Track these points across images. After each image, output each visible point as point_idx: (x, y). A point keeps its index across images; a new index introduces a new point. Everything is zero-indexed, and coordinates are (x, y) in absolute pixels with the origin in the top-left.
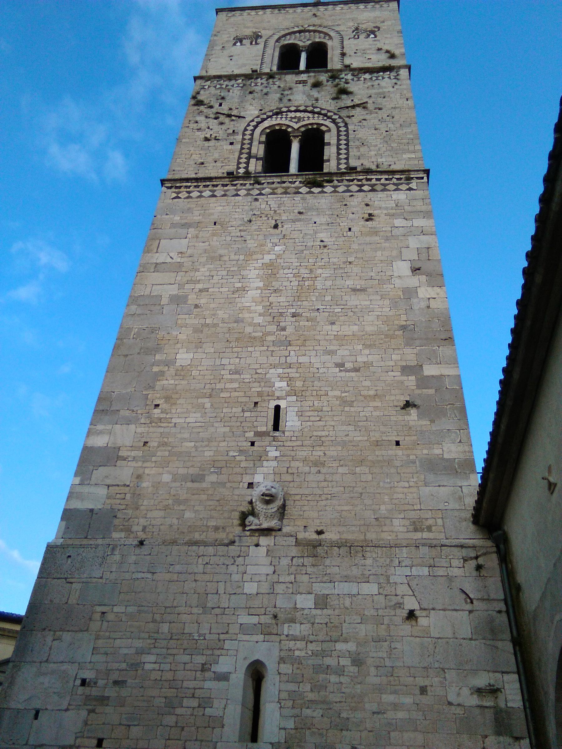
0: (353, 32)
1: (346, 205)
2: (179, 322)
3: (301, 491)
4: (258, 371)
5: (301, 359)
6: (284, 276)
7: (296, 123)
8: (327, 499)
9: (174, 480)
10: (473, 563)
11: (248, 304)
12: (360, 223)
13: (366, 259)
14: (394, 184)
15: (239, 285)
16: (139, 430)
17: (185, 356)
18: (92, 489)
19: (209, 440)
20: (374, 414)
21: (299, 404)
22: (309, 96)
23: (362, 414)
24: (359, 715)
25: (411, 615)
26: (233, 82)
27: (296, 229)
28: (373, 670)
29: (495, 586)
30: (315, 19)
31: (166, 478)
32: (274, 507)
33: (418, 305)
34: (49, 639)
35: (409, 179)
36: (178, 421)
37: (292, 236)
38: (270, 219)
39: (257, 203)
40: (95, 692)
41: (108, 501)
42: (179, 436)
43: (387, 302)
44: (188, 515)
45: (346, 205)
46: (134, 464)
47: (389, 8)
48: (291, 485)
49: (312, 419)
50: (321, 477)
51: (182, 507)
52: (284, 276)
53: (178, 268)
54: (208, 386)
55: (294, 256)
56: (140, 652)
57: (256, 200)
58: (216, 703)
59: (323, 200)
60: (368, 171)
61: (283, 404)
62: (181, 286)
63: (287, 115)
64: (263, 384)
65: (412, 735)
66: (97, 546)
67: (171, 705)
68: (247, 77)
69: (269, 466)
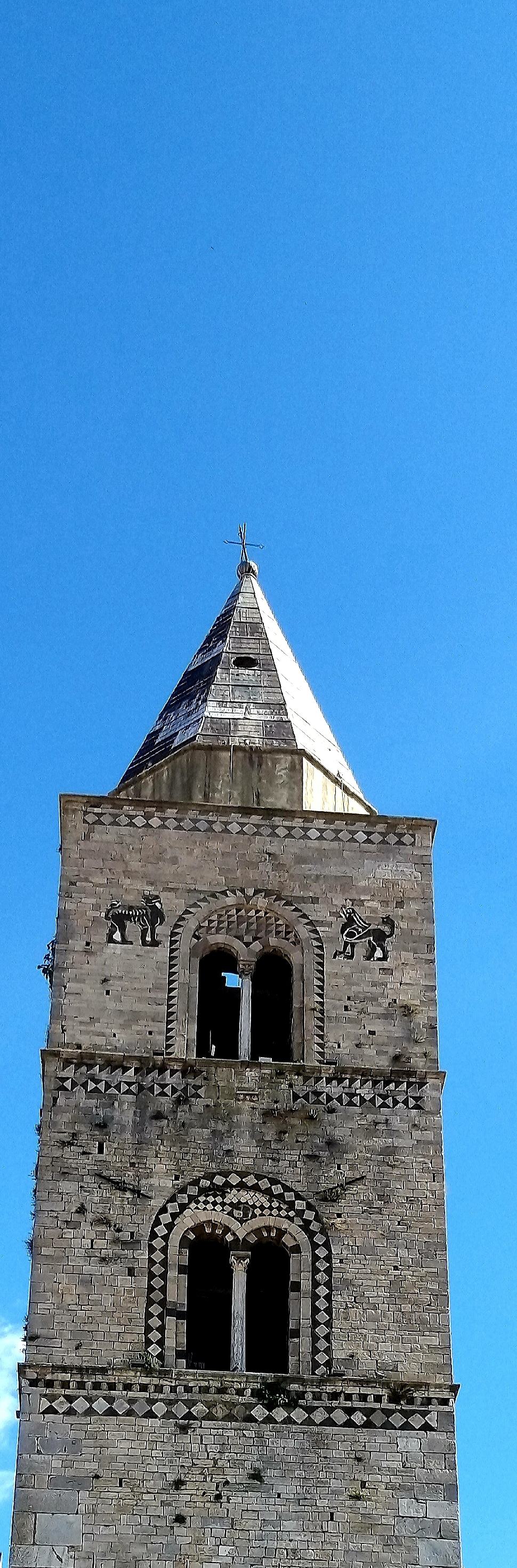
0: (342, 932)
7: (241, 1221)
26: (118, 1076)
68: (145, 1066)
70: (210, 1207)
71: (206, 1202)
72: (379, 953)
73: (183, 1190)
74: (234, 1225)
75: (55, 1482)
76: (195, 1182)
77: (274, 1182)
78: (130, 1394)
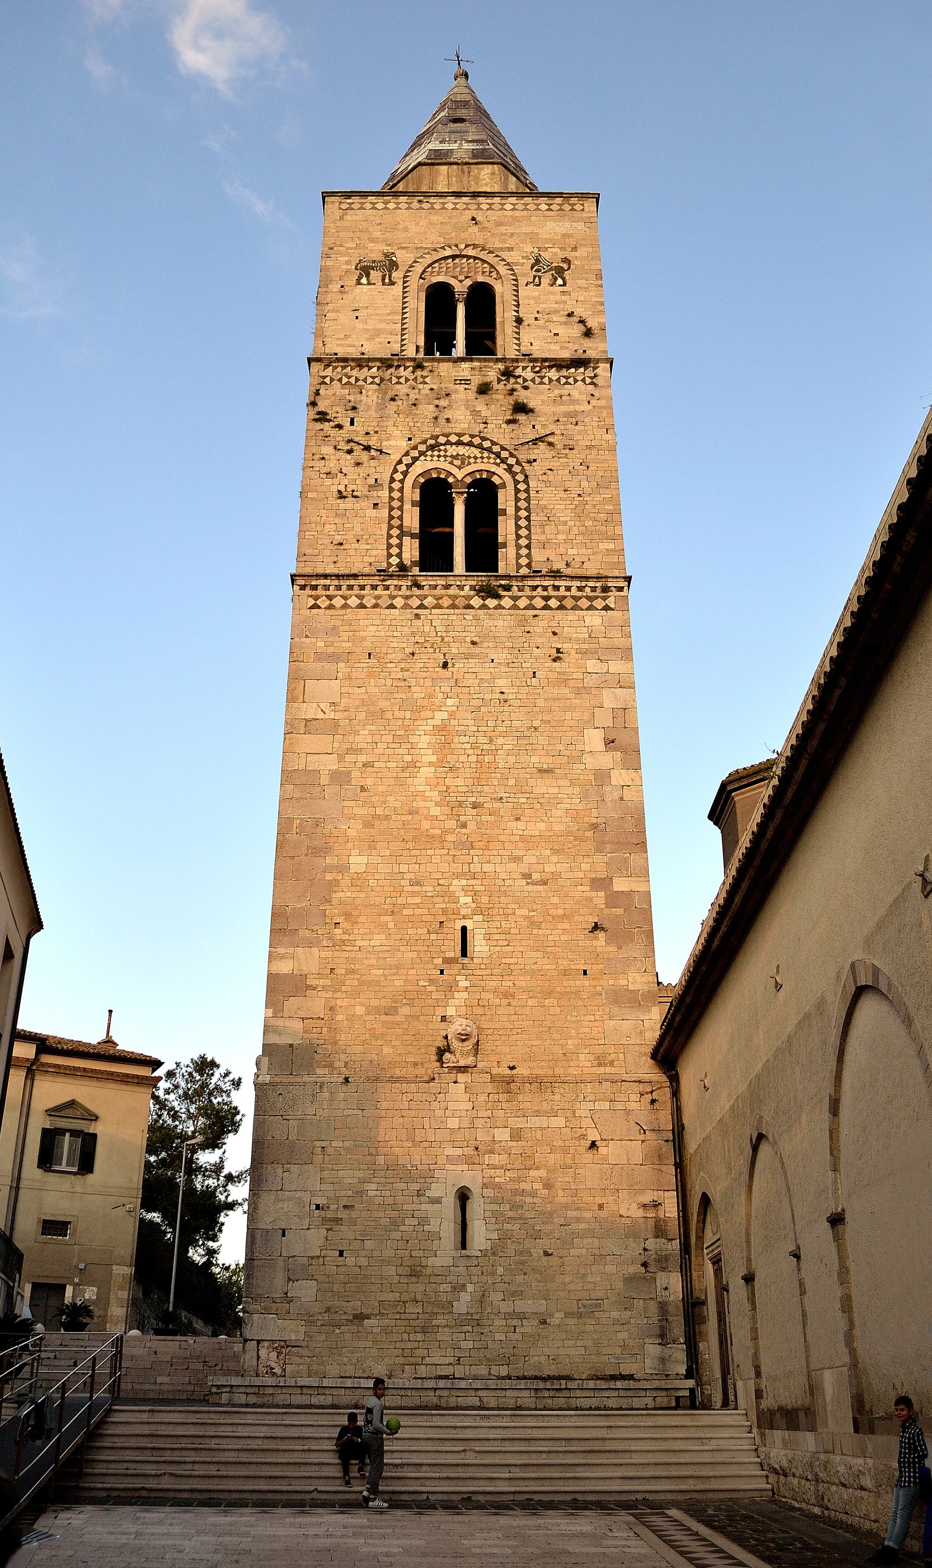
0: (532, 269)
1: (529, 632)
2: (346, 810)
3: (493, 1025)
4: (441, 882)
5: (487, 868)
6: (460, 746)
7: (460, 468)
8: (518, 1033)
9: (368, 1013)
10: (649, 1097)
11: (421, 788)
12: (546, 665)
13: (554, 724)
14: (588, 598)
15: (408, 758)
16: (323, 954)
17: (359, 859)
18: (288, 1023)
19: (397, 967)
20: (563, 938)
21: (486, 925)
22: (475, 413)
23: (551, 938)
24: (549, 1227)
25: (593, 1145)
27: (470, 670)
28: (560, 1193)
29: (665, 1119)
30: (475, 229)
31: (360, 1010)
32: (469, 1045)
33: (612, 795)
34: (279, 1171)
35: (606, 589)
36: (363, 943)
37: (466, 683)
38: (437, 651)
39: (418, 623)
40: (329, 1215)
41: (306, 1036)
42: (365, 962)
43: (577, 790)
44: (386, 1050)
45: (529, 632)
46: (324, 994)
47: (584, 215)
48: (483, 1018)
49: (501, 943)
50: (511, 1010)
51: (380, 1042)
52: (460, 746)
53: (333, 727)
54: (388, 900)
55: (469, 716)
56: (362, 1182)
57: (417, 616)
58: (432, 1221)
59: (498, 620)
60: (556, 574)
61: (469, 925)
62: (341, 758)
63: (446, 451)
64: (446, 899)
65: (590, 1240)
66: (305, 1084)
67: (395, 1224)
68: (386, 363)
69: (461, 997)
70: (435, 458)
71: (432, 456)
72: (560, 281)
73: (415, 448)
74: (454, 471)
75: (319, 657)
76: (424, 442)
77: (484, 439)
78: (376, 593)
